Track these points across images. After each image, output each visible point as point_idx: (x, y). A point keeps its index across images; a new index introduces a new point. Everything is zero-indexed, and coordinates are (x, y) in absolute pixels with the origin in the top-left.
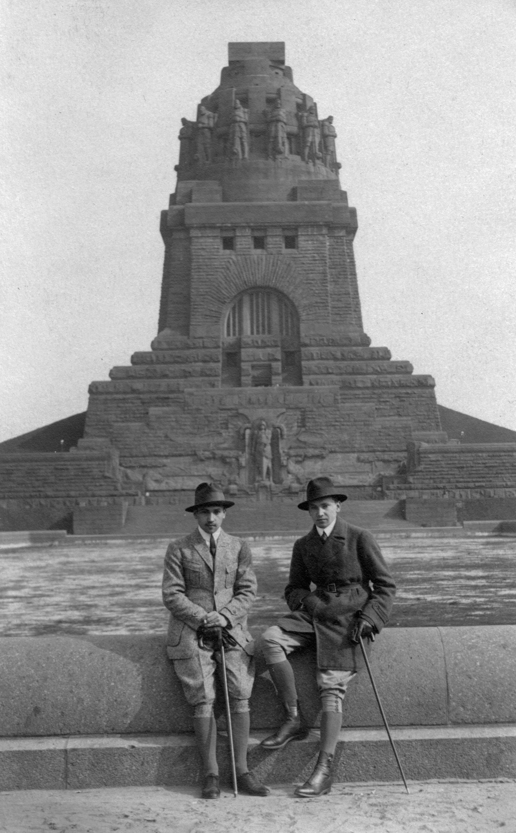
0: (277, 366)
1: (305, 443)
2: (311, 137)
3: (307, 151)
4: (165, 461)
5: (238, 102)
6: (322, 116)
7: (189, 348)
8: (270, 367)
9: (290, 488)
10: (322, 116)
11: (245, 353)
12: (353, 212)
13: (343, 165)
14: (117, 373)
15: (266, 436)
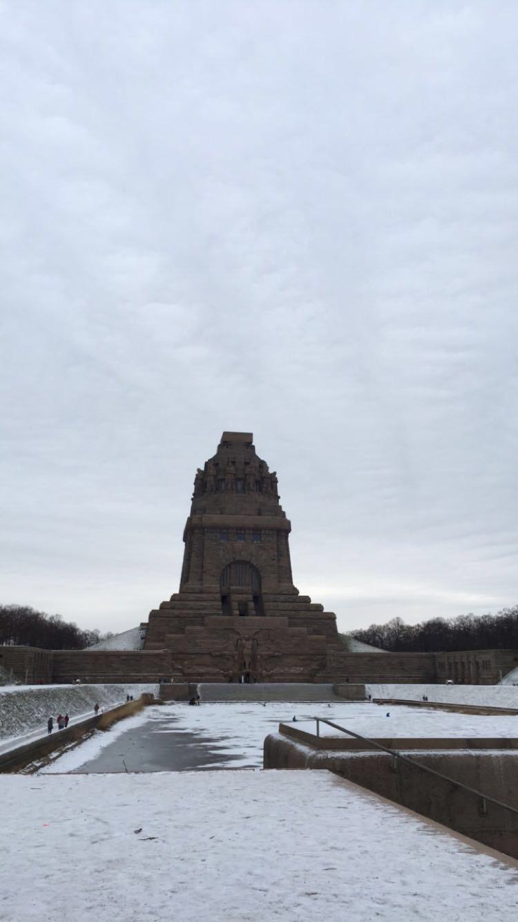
0: (252, 605)
1: (269, 648)
2: (265, 483)
3: (264, 490)
4: (194, 656)
5: (230, 463)
6: (271, 471)
7: (201, 592)
8: (246, 605)
9: (261, 674)
10: (271, 471)
11: (234, 597)
12: (289, 523)
13: (281, 497)
14: (164, 605)
15: (249, 644)
